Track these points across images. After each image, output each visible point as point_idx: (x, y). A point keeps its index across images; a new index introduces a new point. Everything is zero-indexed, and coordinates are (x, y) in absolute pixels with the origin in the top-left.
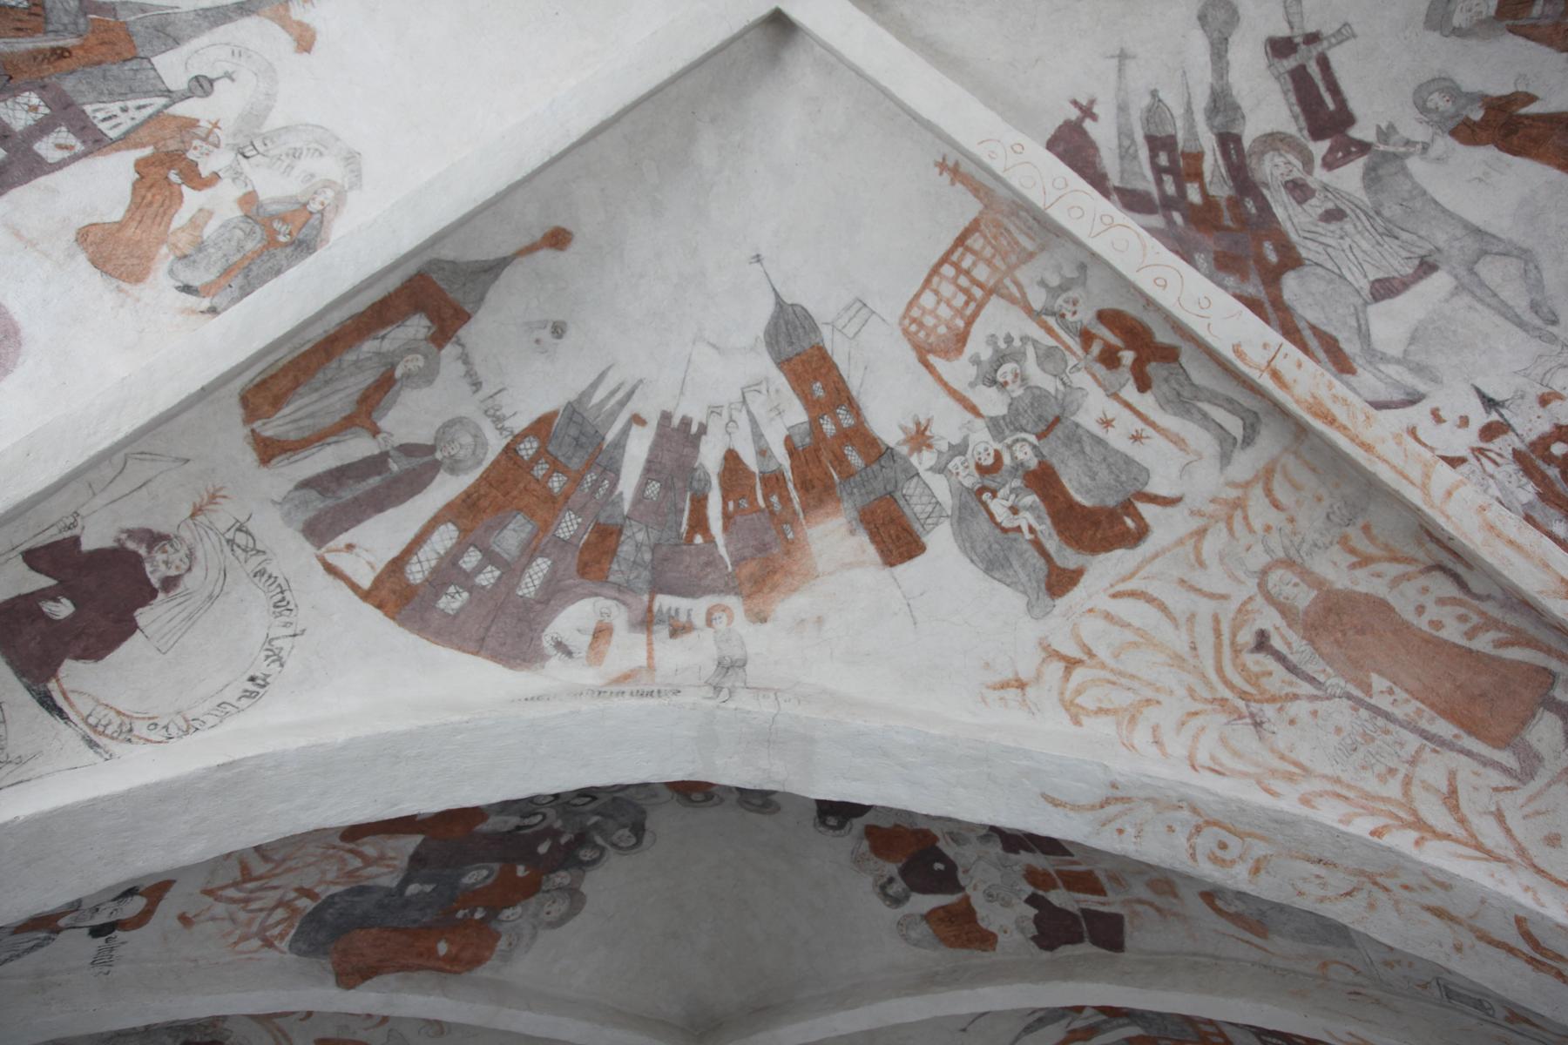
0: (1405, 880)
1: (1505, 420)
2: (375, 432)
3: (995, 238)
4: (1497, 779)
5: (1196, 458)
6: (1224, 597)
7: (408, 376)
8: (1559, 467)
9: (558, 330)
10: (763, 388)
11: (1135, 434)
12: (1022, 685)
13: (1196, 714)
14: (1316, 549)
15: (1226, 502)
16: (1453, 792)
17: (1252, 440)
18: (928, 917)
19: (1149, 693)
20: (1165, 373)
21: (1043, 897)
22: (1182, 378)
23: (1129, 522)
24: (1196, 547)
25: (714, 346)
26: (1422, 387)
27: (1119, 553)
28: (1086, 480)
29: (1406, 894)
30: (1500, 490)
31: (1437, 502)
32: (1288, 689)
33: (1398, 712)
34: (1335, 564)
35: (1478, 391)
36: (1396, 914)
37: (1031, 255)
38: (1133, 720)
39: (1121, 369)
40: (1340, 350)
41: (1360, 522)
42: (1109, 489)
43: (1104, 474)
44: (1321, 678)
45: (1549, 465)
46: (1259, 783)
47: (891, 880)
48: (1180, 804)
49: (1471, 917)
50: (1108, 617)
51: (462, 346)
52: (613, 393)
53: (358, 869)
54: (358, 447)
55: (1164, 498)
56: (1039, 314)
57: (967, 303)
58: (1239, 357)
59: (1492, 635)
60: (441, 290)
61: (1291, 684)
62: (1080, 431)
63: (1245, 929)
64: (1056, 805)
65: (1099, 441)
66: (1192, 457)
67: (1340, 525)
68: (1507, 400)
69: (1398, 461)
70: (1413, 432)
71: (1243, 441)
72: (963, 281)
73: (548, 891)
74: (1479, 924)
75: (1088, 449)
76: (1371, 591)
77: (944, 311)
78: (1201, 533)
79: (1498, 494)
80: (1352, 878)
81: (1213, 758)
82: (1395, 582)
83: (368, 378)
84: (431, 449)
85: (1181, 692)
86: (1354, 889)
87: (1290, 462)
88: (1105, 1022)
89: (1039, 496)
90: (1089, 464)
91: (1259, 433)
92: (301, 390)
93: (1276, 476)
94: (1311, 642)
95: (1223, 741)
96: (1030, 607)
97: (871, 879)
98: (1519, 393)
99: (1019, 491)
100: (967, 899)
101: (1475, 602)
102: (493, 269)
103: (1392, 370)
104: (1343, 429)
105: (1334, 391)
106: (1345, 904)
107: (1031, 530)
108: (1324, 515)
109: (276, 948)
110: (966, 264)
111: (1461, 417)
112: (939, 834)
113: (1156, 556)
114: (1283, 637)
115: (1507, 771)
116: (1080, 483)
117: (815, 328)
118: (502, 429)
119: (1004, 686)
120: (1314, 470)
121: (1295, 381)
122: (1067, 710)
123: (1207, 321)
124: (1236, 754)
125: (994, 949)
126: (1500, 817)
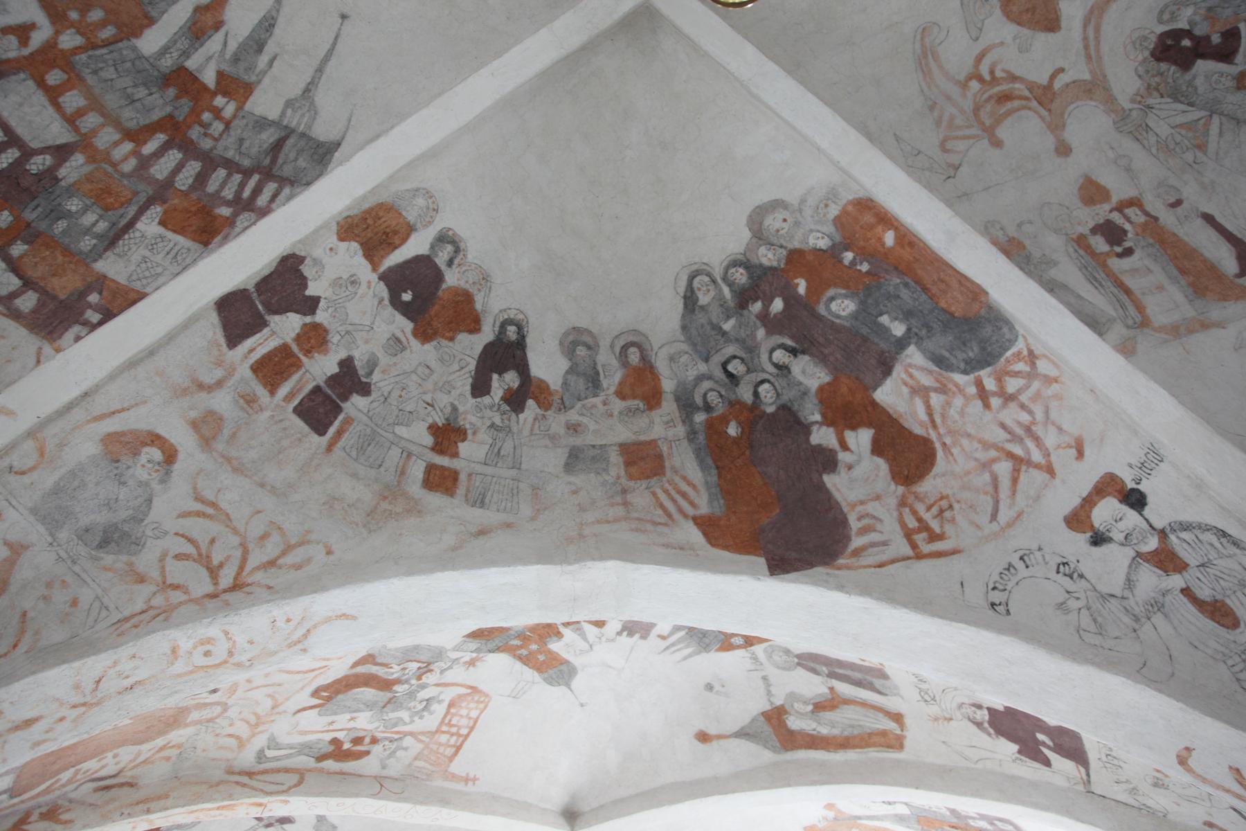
0: (66, 724)
2: (832, 689)
3: (439, 758)
7: (805, 703)
9: (710, 687)
10: (578, 652)
15: (264, 723)
18: (410, 229)
21: (305, 315)
23: (325, 694)
25: (610, 667)
27: (330, 680)
29: (59, 715)
37: (416, 759)
47: (450, 263)
50: (328, 660)
51: (769, 701)
52: (678, 650)
53: (936, 390)
54: (844, 689)
56: (405, 736)
57: (450, 720)
59: (63, 781)
60: (776, 736)
63: (123, 434)
64: (344, 615)
72: (454, 730)
73: (781, 247)
77: (464, 712)
80: (102, 695)
82: (138, 755)
83: (828, 715)
84: (799, 664)
86: (96, 689)
88: (186, 54)
92: (869, 731)
97: (470, 257)
100: (374, 269)
102: (742, 734)
104: (210, 810)
106: (96, 674)
109: (1028, 345)
110: (454, 739)
112: (415, 343)
113: (302, 689)
117: (545, 680)
118: (753, 654)
120: (213, 760)
125: (338, 223)
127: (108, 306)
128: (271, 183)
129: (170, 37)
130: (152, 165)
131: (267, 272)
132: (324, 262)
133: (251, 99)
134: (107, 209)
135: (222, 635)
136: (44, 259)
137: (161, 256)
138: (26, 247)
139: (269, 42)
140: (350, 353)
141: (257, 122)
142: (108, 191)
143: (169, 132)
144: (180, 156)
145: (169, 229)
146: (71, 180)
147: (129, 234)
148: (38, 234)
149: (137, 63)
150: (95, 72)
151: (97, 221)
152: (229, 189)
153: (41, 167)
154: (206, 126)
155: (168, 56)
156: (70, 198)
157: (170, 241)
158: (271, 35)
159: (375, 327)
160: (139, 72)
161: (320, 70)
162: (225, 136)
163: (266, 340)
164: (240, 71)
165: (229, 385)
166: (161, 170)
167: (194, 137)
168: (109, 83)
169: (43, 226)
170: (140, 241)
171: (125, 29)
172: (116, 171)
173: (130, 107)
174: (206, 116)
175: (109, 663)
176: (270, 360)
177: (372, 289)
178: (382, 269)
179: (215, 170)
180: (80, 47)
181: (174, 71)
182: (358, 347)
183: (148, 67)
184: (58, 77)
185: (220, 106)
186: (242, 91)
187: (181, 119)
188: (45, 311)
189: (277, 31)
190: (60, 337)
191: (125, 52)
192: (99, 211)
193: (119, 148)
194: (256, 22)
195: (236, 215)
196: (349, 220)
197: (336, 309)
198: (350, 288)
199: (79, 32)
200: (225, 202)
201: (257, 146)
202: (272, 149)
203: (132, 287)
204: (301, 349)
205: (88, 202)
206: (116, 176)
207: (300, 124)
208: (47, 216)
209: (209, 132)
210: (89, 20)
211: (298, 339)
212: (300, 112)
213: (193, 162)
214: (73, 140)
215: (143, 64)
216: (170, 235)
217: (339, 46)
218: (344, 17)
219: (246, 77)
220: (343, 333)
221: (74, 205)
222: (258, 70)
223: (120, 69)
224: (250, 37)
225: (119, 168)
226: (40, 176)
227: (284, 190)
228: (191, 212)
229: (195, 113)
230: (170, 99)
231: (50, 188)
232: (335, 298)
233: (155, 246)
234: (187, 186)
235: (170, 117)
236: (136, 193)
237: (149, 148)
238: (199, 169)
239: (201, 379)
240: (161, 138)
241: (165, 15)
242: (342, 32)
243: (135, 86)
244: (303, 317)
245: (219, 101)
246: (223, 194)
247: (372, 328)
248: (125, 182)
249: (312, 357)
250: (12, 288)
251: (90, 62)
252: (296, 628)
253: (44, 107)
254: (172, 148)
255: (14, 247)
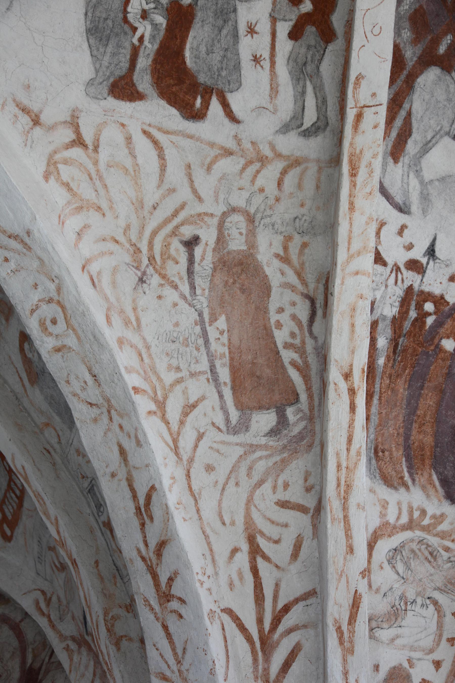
0: (125, 423)
1: (427, 267)
4: (220, 420)
5: (272, 110)
6: (200, 199)
8: (418, 314)
11: (258, 56)
12: (36, 122)
13: (117, 242)
14: (271, 227)
16: (194, 406)
17: (309, 136)
19: (104, 205)
20: (313, 43)
22: (317, 57)
23: (199, 101)
24: (216, 157)
26: (414, 208)
27: (174, 111)
28: (203, 49)
29: (117, 429)
30: (382, 297)
31: (347, 271)
32: (176, 280)
33: (214, 346)
34: (271, 244)
35: (434, 240)
36: (103, 434)
38: (80, 209)
39: (295, 9)
40: (406, 142)
41: (306, 239)
42: (209, 70)
43: (216, 57)
44: (198, 292)
45: (416, 309)
46: (108, 309)
48: (55, 279)
49: (134, 467)
50: (129, 139)
55: (232, 111)
58: (355, 84)
59: (296, 356)
61: (181, 278)
62: (232, 16)
65: (236, 36)
66: (270, 107)
67: (296, 230)
68: (439, 259)
69: (356, 231)
70: (382, 224)
71: (304, 131)
74: (135, 474)
75: (224, 32)
76: (270, 277)
78: (228, 153)
79: (378, 297)
80: (100, 398)
81: (99, 273)
85: (122, 223)
87: (313, 169)
89: (167, 25)
90: (216, 42)
91: (316, 136)
93: (298, 168)
94: (215, 269)
95: (115, 271)
96: (90, 83)
98: (448, 262)
99: (159, 7)
101: (307, 334)
103: (414, 183)
104: (354, 185)
105: (373, 160)
106: (84, 408)
107: (141, 39)
108: (295, 216)
111: (411, 243)
113: (191, 137)
114: (204, 252)
115: (228, 421)
116: (198, 47)
119: (25, 110)
120: (318, 187)
121: (364, 132)
122: (48, 165)
123: (365, 42)
124: (114, 284)
126: (200, 437)
135: (35, 314)
175: (75, 400)
252: (13, 250)
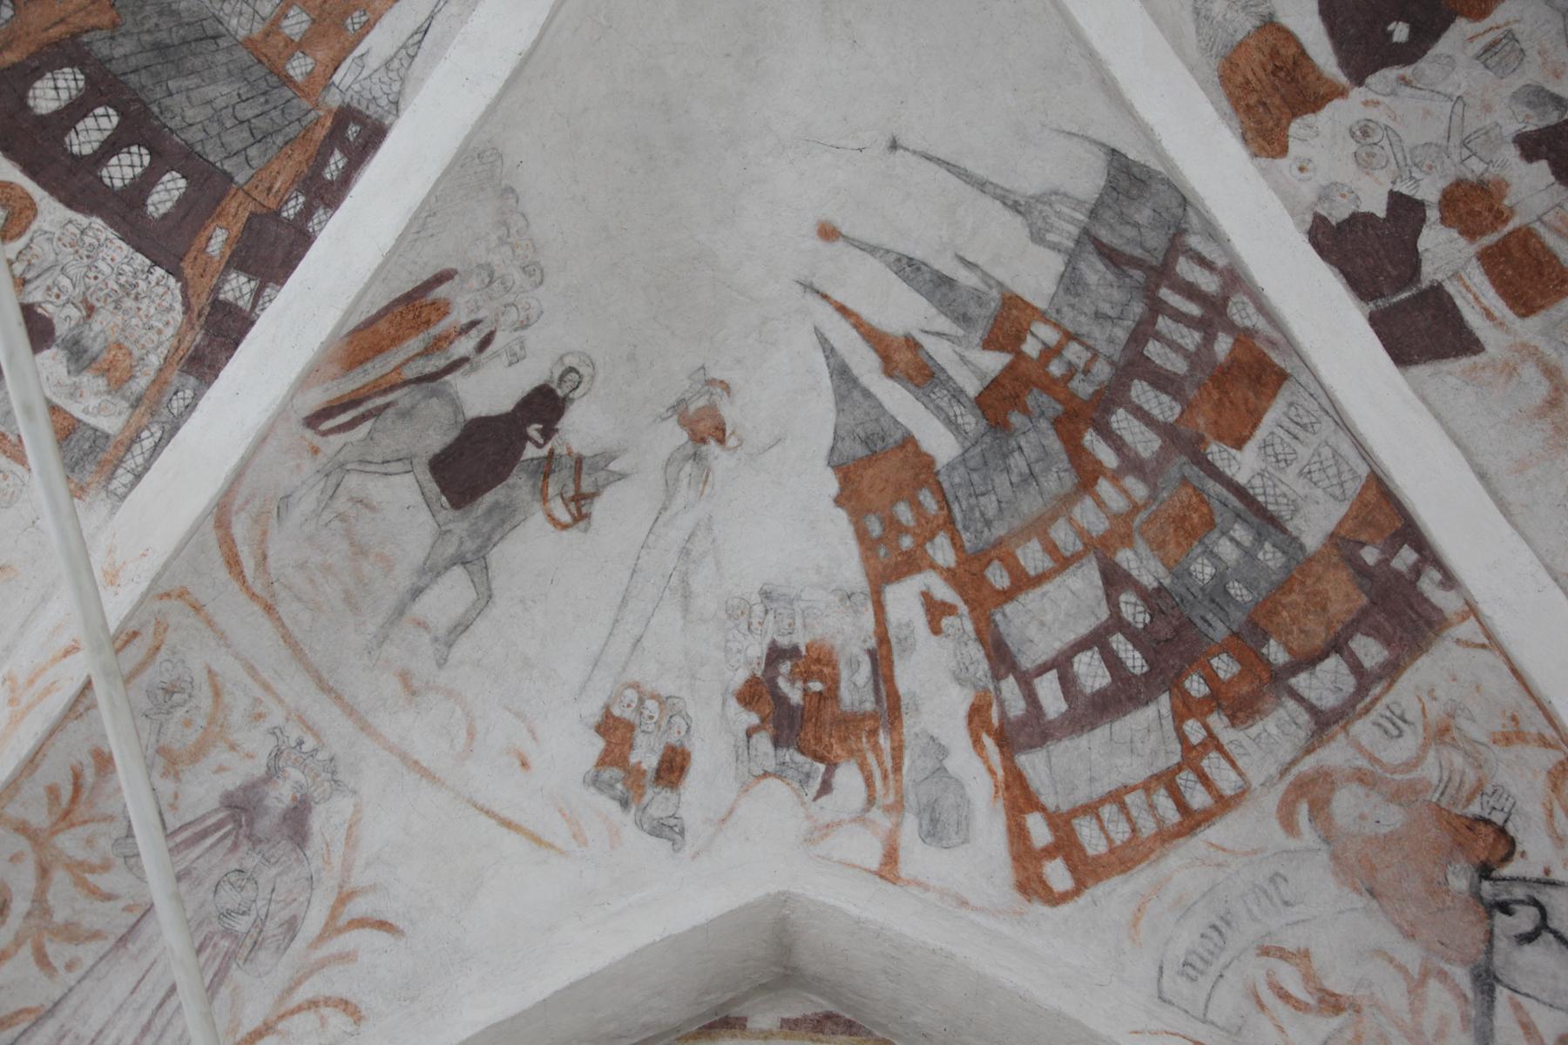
21: (1423, 220)
88: (957, 394)
100: (1342, 93)
112: (1499, 16)
127: (1387, 535)
128: (1178, 269)
129: (932, 416)
130: (1137, 453)
131: (1344, 281)
132: (1325, 183)
133: (1028, 298)
134: (1211, 525)
136: (1294, 620)
137: (1299, 448)
138: (1272, 642)
139: (936, 267)
140: (1510, 139)
141: (1067, 290)
142: (1180, 522)
143: (1082, 426)
144: (1121, 412)
145: (1251, 434)
146: (1161, 571)
147: (1255, 495)
148: (1252, 623)
149: (972, 464)
150: (988, 523)
151: (1232, 539)
152: (1183, 337)
153: (1140, 609)
154: (1072, 370)
155: (960, 420)
156: (1190, 574)
157: (1272, 433)
158: (926, 265)
159: (1458, 94)
160: (986, 464)
161: (982, 185)
162: (1091, 342)
163: (1467, 288)
164: (983, 315)
165: (1554, 356)
166: (1145, 443)
167: (1091, 390)
168: (1003, 505)
169: (1238, 616)
170: (1270, 479)
171: (923, 477)
172: (1145, 506)
173: (1042, 479)
174: (1056, 369)
176: (1510, 284)
177: (1380, 98)
178: (1342, 79)
179: (1148, 358)
180: (952, 539)
181: (983, 413)
182: (1497, 124)
183: (978, 449)
184: (998, 572)
185: (1040, 346)
186: (1015, 312)
187: (1059, 407)
188: (1390, 629)
189: (918, 254)
190: (1440, 611)
191: (957, 480)
192: (1215, 535)
193: (1107, 500)
194: (905, 285)
195: (1231, 327)
196: (1249, 135)
197: (1416, 165)
198: (1376, 141)
199: (931, 538)
200: (1205, 346)
201: (1109, 291)
202: (1116, 265)
203: (1355, 496)
204: (1494, 229)
205: (1199, 550)
206: (1154, 508)
207: (1074, 219)
208: (1222, 608)
209: (1082, 365)
210: (912, 524)
211: (1470, 234)
212: (1054, 219)
213: (1133, 393)
214: (1094, 563)
215: (973, 457)
216: (1261, 434)
217: (941, 153)
218: (894, 146)
219: (993, 305)
220: (1466, 152)
221: (1203, 571)
222: (982, 287)
223: (982, 489)
224: (929, 296)
225: (1140, 503)
226: (1155, 611)
227: (1193, 246)
228: (1220, 399)
229: (1049, 386)
230: (1026, 421)
231: (1174, 599)
232: (1393, 166)
233: (1280, 457)
234: (1174, 403)
235: (1056, 423)
236: (1185, 481)
237: (1107, 457)
238: (1145, 384)
239: (1538, 401)
240: (1090, 438)
241: (899, 419)
242: (919, 149)
243: (1008, 470)
244: (1428, 223)
245: (1031, 348)
246: (1191, 348)
247: (1459, 97)
248: (1165, 494)
249: (1512, 210)
250: (1344, 669)
251: (972, 529)
253: (1044, 594)
254: (1108, 423)
255: (1272, 658)
